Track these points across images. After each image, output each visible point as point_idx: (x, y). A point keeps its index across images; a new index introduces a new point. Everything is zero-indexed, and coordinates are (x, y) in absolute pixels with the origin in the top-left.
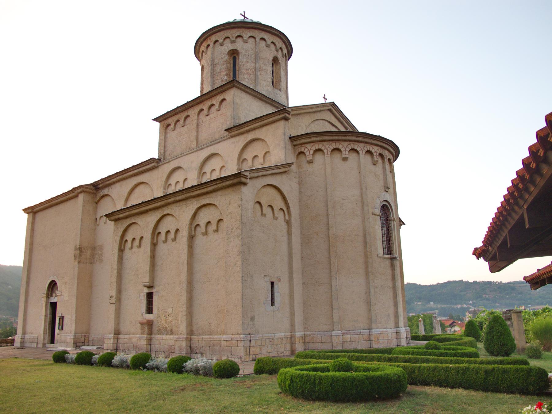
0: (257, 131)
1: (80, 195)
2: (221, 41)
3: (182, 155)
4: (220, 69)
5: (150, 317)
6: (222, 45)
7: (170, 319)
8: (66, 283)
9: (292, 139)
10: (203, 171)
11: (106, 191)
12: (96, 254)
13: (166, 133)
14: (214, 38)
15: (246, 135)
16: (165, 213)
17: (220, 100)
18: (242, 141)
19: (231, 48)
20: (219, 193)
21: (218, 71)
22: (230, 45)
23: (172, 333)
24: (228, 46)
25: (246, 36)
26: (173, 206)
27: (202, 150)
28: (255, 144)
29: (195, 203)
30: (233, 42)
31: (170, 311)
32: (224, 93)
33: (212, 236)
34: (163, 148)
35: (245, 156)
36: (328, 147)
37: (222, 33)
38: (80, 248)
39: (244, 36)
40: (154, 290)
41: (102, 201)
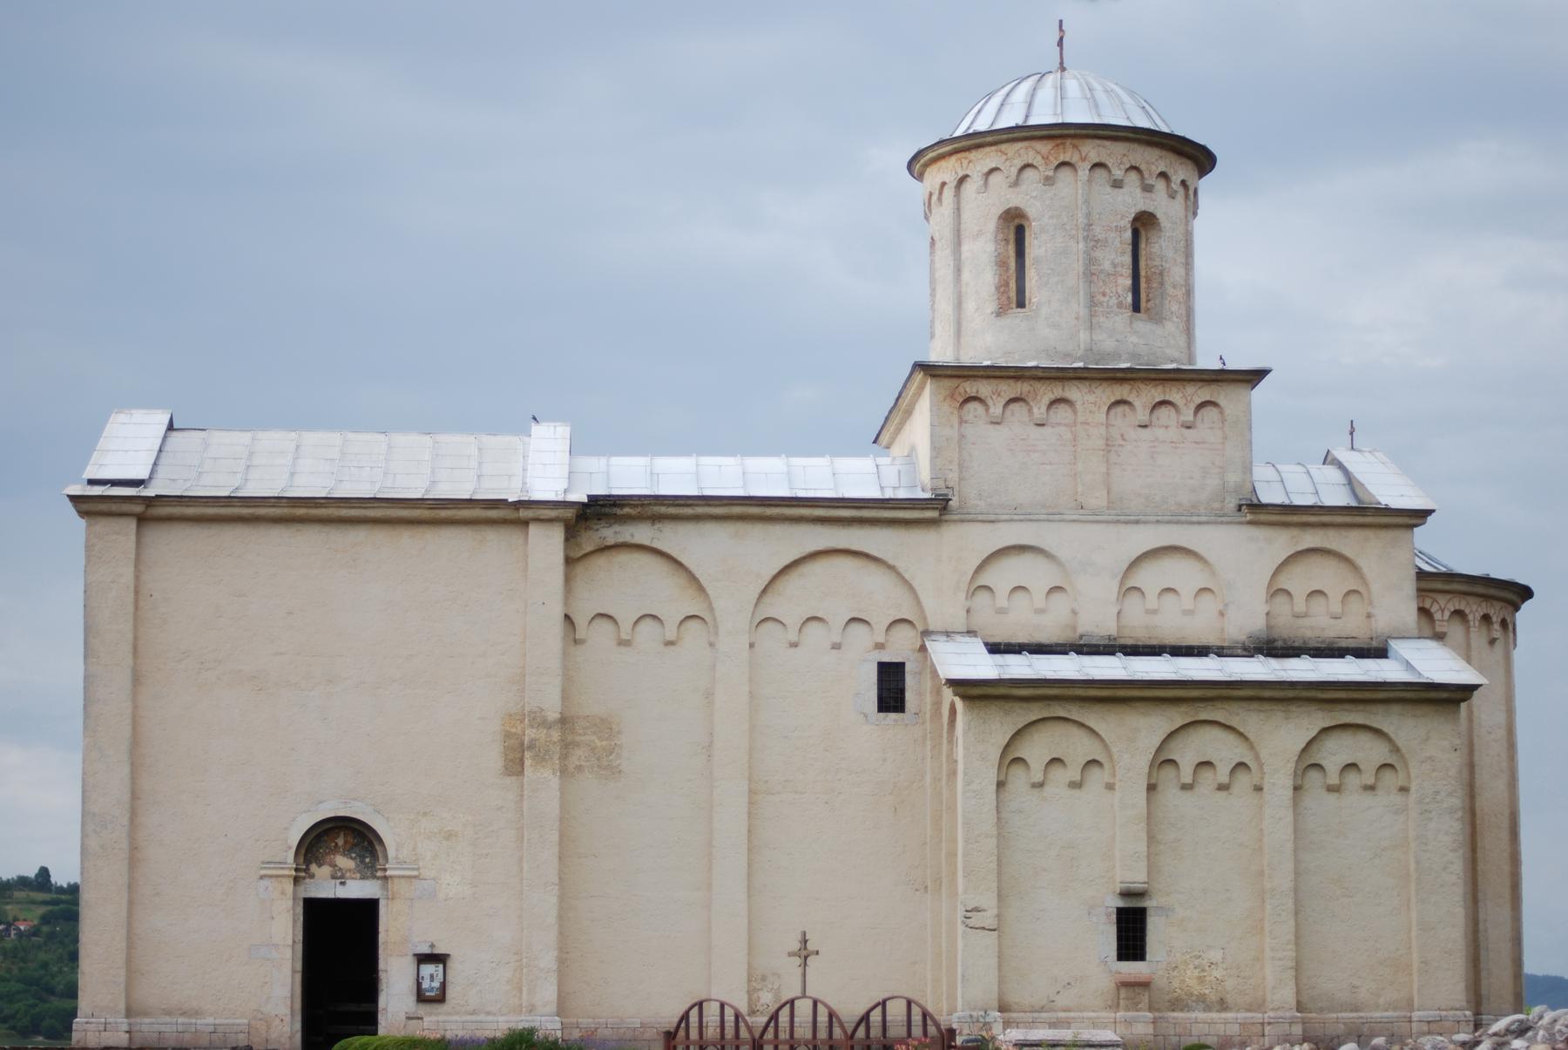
0: (1331, 533)
1: (533, 529)
2: (1118, 173)
3: (1052, 515)
4: (1115, 266)
5: (1132, 969)
6: (1117, 184)
7: (1217, 973)
8: (450, 836)
9: (1421, 575)
10: (1130, 584)
11: (641, 533)
12: (578, 745)
13: (962, 421)
14: (1093, 151)
15: (1295, 532)
16: (1203, 716)
17: (1199, 401)
18: (1282, 543)
19: (1141, 207)
20: (1396, 708)
21: (1107, 266)
22: (1138, 191)
23: (1223, 1005)
24: (1131, 200)
25: (1176, 179)
26: (1234, 707)
27: (1136, 527)
28: (1316, 563)
29: (1320, 714)
30: (1148, 189)
31: (1216, 955)
32: (1214, 387)
33: (1354, 800)
34: (955, 467)
35: (1284, 582)
36: (1475, 610)
37: (1119, 148)
38: (564, 721)
39: (1173, 178)
40: (1146, 903)
41: (601, 561)
